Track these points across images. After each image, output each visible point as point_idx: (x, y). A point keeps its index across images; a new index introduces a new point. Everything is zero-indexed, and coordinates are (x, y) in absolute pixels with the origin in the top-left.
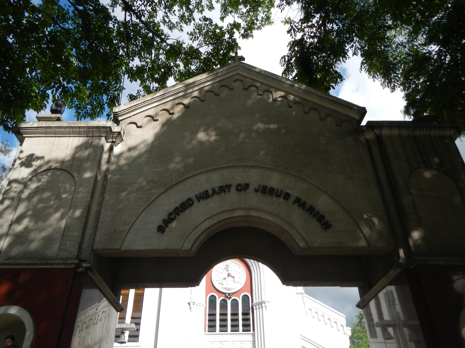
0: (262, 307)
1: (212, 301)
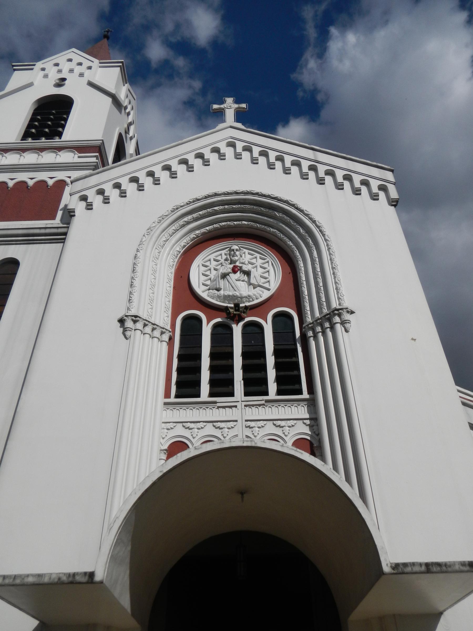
0: (332, 328)
1: (191, 328)
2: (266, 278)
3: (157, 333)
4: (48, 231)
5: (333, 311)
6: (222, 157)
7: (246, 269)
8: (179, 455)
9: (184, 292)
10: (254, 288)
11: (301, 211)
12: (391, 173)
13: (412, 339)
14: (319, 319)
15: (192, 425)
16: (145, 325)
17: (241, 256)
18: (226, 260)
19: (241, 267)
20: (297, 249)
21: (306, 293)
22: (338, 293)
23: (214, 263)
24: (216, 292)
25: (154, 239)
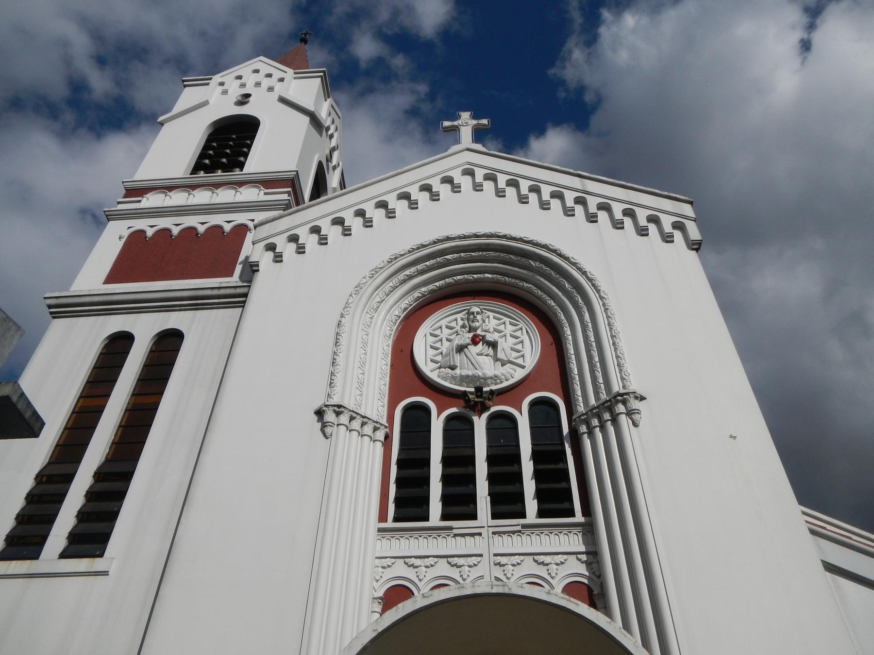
0: (615, 420)
1: (415, 423)
2: (518, 351)
3: (368, 430)
4: (222, 292)
5: (615, 397)
6: (456, 188)
7: (491, 339)
8: (400, 605)
9: (405, 371)
10: (503, 365)
11: (566, 259)
12: (690, 206)
13: (731, 436)
14: (595, 408)
15: (417, 562)
16: (352, 419)
17: (484, 322)
18: (463, 326)
19: (484, 337)
20: (562, 310)
21: (576, 371)
22: (621, 371)
23: (446, 332)
24: (450, 371)
25: (364, 300)
